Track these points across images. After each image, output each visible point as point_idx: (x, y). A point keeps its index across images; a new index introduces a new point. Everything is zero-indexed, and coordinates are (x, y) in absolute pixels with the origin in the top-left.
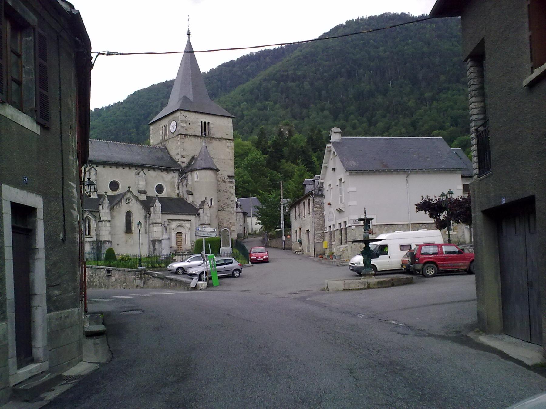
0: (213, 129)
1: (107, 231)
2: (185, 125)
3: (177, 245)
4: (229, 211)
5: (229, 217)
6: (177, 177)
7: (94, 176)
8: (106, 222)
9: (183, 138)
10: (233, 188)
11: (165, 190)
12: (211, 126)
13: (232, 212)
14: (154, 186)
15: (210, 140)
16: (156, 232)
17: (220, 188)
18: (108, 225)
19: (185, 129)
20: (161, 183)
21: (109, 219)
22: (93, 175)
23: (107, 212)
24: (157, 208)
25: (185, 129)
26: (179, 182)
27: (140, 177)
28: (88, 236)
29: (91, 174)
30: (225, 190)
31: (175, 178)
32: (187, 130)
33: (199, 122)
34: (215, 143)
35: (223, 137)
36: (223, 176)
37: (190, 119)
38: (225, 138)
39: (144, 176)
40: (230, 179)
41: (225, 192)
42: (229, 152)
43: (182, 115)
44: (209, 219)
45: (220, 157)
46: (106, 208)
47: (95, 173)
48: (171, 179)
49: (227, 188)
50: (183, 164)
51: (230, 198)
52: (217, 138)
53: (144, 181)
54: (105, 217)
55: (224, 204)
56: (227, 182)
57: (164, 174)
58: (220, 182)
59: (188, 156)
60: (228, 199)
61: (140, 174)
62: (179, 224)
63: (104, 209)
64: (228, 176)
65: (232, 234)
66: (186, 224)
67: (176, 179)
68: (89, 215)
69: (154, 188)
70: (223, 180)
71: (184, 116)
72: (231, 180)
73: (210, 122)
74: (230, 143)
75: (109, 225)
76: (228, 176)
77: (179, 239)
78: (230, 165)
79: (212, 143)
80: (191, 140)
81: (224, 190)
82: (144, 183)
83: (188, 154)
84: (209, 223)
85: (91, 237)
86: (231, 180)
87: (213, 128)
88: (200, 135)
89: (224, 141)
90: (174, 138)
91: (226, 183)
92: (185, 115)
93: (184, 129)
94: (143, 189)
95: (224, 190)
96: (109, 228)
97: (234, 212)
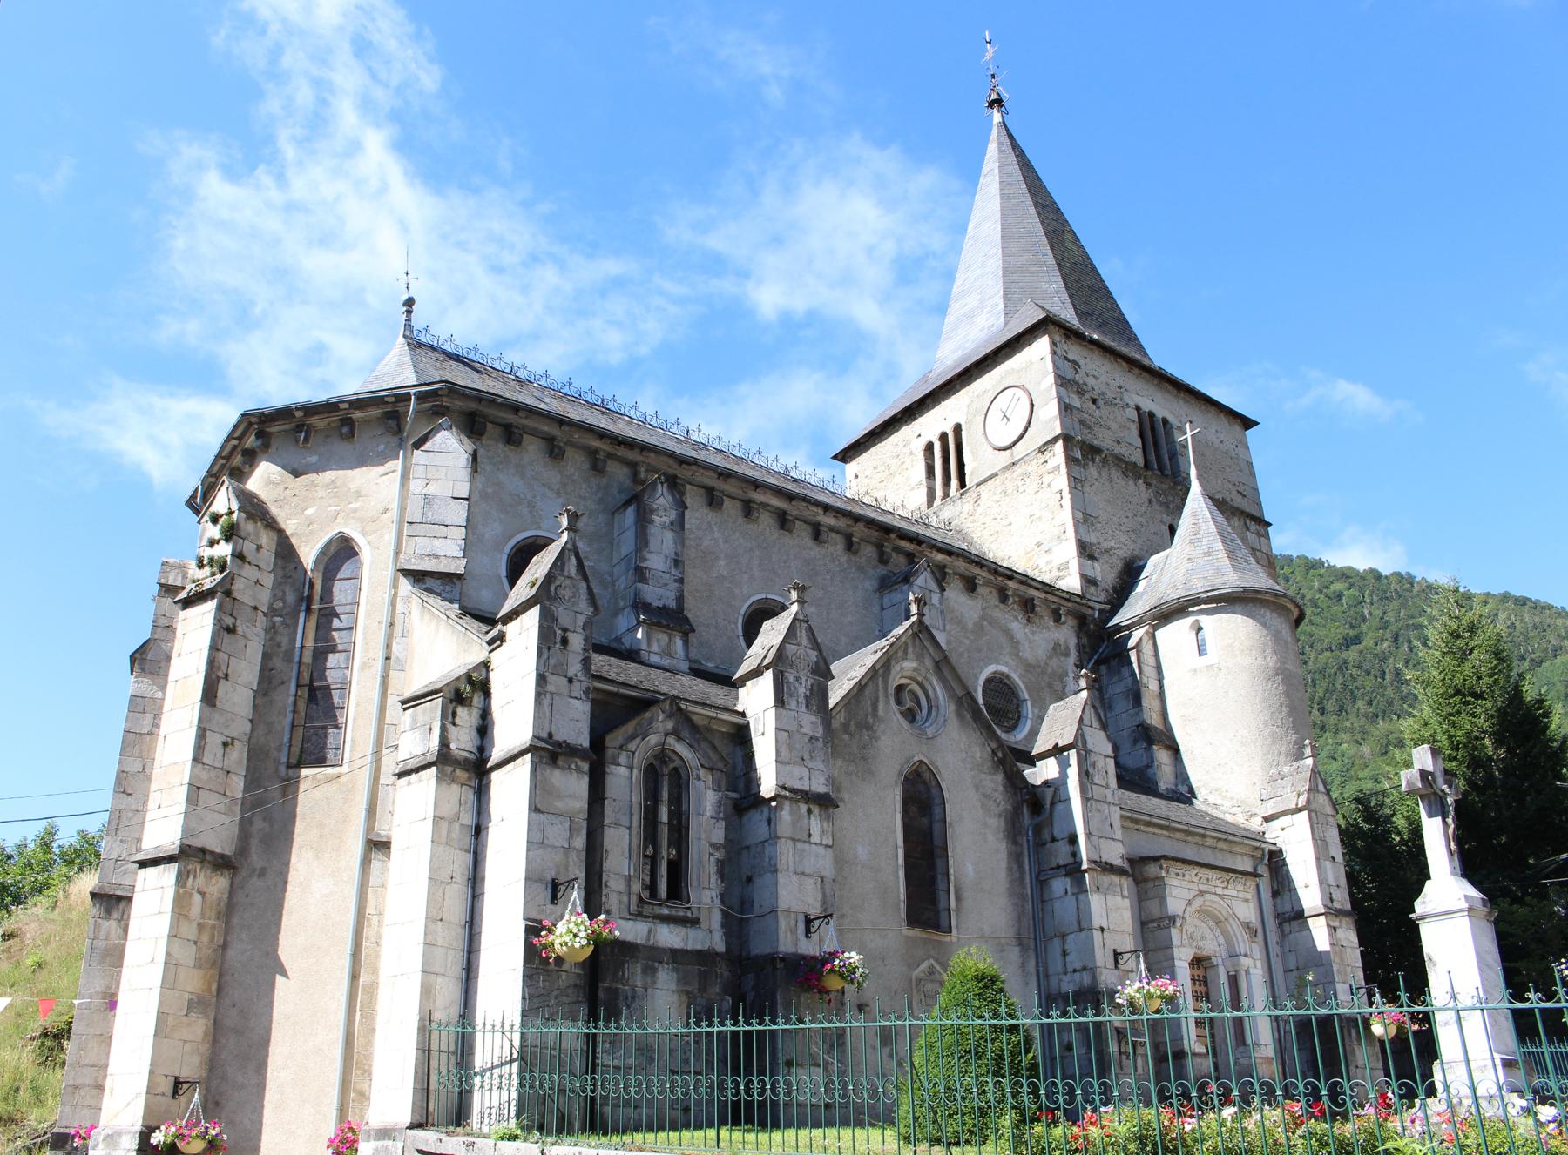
1: (811, 880)
7: (669, 536)
8: (803, 808)
16: (1102, 930)
18: (815, 838)
20: (1004, 669)
22: (663, 526)
28: (665, 911)
32: (1089, 428)
37: (1091, 381)
46: (802, 699)
47: (673, 515)
62: (1201, 893)
63: (793, 705)
66: (1234, 903)
71: (1066, 358)
85: (694, 922)
88: (1141, 462)
90: (1018, 470)
92: (1071, 357)
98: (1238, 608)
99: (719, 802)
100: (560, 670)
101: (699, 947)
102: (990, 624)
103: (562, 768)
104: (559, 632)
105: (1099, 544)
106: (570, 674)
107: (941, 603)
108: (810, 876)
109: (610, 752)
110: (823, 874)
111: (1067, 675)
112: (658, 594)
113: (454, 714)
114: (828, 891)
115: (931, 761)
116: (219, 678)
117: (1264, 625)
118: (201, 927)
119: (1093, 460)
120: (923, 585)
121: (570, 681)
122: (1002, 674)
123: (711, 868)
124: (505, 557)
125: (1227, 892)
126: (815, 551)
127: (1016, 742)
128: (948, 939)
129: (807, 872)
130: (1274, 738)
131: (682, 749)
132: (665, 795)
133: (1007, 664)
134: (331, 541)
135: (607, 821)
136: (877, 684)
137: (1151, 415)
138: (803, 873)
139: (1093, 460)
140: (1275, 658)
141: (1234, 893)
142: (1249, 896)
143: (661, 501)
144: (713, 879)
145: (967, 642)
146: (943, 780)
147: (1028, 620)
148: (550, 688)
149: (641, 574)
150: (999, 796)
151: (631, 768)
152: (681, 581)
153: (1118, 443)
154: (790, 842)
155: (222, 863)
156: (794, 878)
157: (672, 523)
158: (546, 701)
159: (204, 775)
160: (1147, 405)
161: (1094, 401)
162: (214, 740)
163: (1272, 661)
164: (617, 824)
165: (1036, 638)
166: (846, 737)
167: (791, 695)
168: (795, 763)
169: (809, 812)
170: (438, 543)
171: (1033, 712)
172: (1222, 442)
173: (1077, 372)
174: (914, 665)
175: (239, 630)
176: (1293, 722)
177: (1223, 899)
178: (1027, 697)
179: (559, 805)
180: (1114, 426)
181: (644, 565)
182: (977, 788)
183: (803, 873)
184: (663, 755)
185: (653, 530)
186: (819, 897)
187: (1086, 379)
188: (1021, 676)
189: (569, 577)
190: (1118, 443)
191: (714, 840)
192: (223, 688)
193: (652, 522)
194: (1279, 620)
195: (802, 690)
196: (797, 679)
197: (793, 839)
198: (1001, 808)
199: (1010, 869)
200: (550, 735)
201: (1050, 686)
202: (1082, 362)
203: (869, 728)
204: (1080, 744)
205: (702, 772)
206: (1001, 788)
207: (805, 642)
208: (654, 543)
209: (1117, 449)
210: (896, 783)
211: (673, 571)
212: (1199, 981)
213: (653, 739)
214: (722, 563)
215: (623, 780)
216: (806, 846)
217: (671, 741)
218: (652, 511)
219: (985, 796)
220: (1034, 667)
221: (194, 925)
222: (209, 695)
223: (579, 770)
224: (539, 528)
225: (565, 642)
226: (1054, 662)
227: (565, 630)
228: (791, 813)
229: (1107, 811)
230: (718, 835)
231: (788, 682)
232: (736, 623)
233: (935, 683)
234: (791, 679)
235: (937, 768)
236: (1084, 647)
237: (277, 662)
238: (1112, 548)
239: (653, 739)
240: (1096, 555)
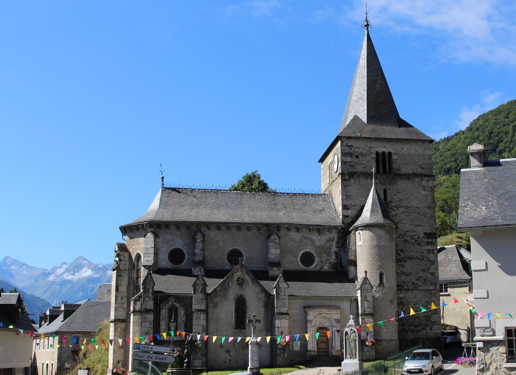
0: (398, 161)
1: (200, 326)
2: (349, 159)
3: (318, 348)
4: (426, 290)
5: (427, 300)
6: (336, 240)
7: (201, 244)
8: (199, 313)
9: (346, 180)
10: (433, 253)
11: (316, 259)
12: (394, 157)
13: (433, 292)
14: (298, 255)
15: (393, 179)
16: (278, 327)
17: (411, 254)
18: (202, 318)
19: (350, 166)
20: (308, 250)
21: (203, 308)
22: (199, 242)
23: (201, 297)
24: (281, 291)
25: (350, 166)
26: (340, 247)
27: (271, 242)
29: (197, 241)
30: (419, 257)
31: (333, 240)
32: (353, 166)
33: (372, 153)
34: (401, 184)
35: (415, 172)
36: (415, 233)
37: (357, 150)
38: (418, 173)
39: (277, 241)
40: (428, 238)
41: (420, 259)
42: (426, 196)
43: (344, 145)
44: (371, 306)
45: (409, 205)
46: (200, 292)
47: (202, 239)
48: (326, 243)
49: (423, 253)
50: (347, 219)
51: (429, 268)
52: (405, 175)
53: (279, 247)
54: (198, 306)
55: (417, 279)
56: (423, 244)
57: (315, 237)
58: (411, 244)
59: (354, 205)
60: (424, 270)
61: (273, 237)
62: (320, 314)
64: (425, 233)
65: (432, 329)
67: (335, 242)
68: (175, 302)
69: (297, 258)
70: (416, 241)
71: (347, 146)
72: (430, 240)
73: (392, 151)
74: (428, 180)
75: (203, 317)
76: (425, 233)
77: (323, 338)
78: (428, 215)
79: (395, 183)
80: (359, 182)
81: (417, 257)
82: (278, 251)
83: (354, 203)
84: (372, 312)
86: (430, 240)
87: (397, 159)
89: (417, 180)
91: (421, 245)
92: (349, 145)
93: (348, 166)
94: (277, 260)
95: (417, 257)
96: (204, 323)
97: (436, 291)
98: (367, 229)
99: (184, 313)
100: (147, 296)
101: (180, 340)
102: (305, 239)
103: (148, 314)
104: (147, 290)
105: (352, 204)
106: (150, 296)
107: (279, 241)
108: (200, 325)
109: (161, 307)
110: (203, 324)
111: (332, 246)
112: (198, 258)
113: (136, 303)
114: (204, 328)
115: (243, 294)
116: (118, 286)
117: (374, 233)
118: (120, 333)
119: (353, 177)
120: (273, 238)
121: (150, 298)
122: (308, 251)
123: (183, 325)
124: (167, 254)
125: (330, 312)
126: (248, 233)
127: (311, 269)
128: (245, 331)
129: (200, 324)
130: (373, 264)
131: (177, 304)
132: (173, 313)
133: (309, 249)
134: (137, 254)
135: (161, 320)
136: (229, 280)
137: (383, 153)
138: (199, 325)
139: (353, 177)
140: (376, 242)
141: (333, 312)
142: (339, 313)
143: (199, 236)
144: (183, 327)
145: (296, 245)
146: (246, 297)
147: (319, 234)
148: (146, 300)
149: (194, 255)
150: (263, 298)
151: (165, 309)
152: (204, 254)
153: (366, 168)
154: (196, 320)
155: (123, 321)
156: (197, 326)
157: (201, 241)
158: (145, 302)
159: (118, 305)
160: (381, 150)
161: (357, 157)
162: (119, 298)
163: (375, 243)
164: (163, 320)
165: (322, 238)
166: (220, 293)
167: (197, 291)
168: (197, 304)
169: (200, 313)
170: (149, 258)
171: (318, 260)
172: (417, 151)
173: (351, 149)
174: (241, 273)
175: (122, 275)
176: (379, 260)
178: (316, 256)
179: (148, 320)
180: (364, 162)
181: (195, 252)
182: (256, 297)
183: (199, 325)
184: (173, 306)
185: (197, 244)
186: (202, 329)
187: (354, 150)
188: (314, 251)
189: (149, 279)
190: (366, 168)
191: (183, 320)
192: (120, 288)
193: (196, 242)
194: (380, 230)
195: (200, 290)
196: (199, 288)
197: (197, 319)
198: (263, 301)
199: (265, 314)
200: (146, 308)
201: (325, 251)
202: (354, 145)
203: (227, 290)
204: (277, 287)
205: (181, 308)
206: (264, 296)
207: (201, 280)
208: (197, 247)
209: (365, 170)
210: (233, 300)
211: (202, 252)
213: (170, 303)
214: (221, 243)
215: (164, 312)
216: (200, 320)
217: (174, 303)
218: (197, 239)
219: (259, 299)
220: (319, 247)
221: (119, 333)
222: (117, 290)
223: (151, 314)
224: (175, 246)
225: (148, 291)
226: (328, 244)
227: (148, 289)
228: (196, 314)
229: (284, 301)
230: (184, 319)
231: (197, 289)
232: (225, 257)
233: (247, 276)
234: (197, 288)
235: (245, 295)
236: (341, 237)
237: (130, 280)
238: (357, 204)
239: (170, 303)
240: (350, 208)
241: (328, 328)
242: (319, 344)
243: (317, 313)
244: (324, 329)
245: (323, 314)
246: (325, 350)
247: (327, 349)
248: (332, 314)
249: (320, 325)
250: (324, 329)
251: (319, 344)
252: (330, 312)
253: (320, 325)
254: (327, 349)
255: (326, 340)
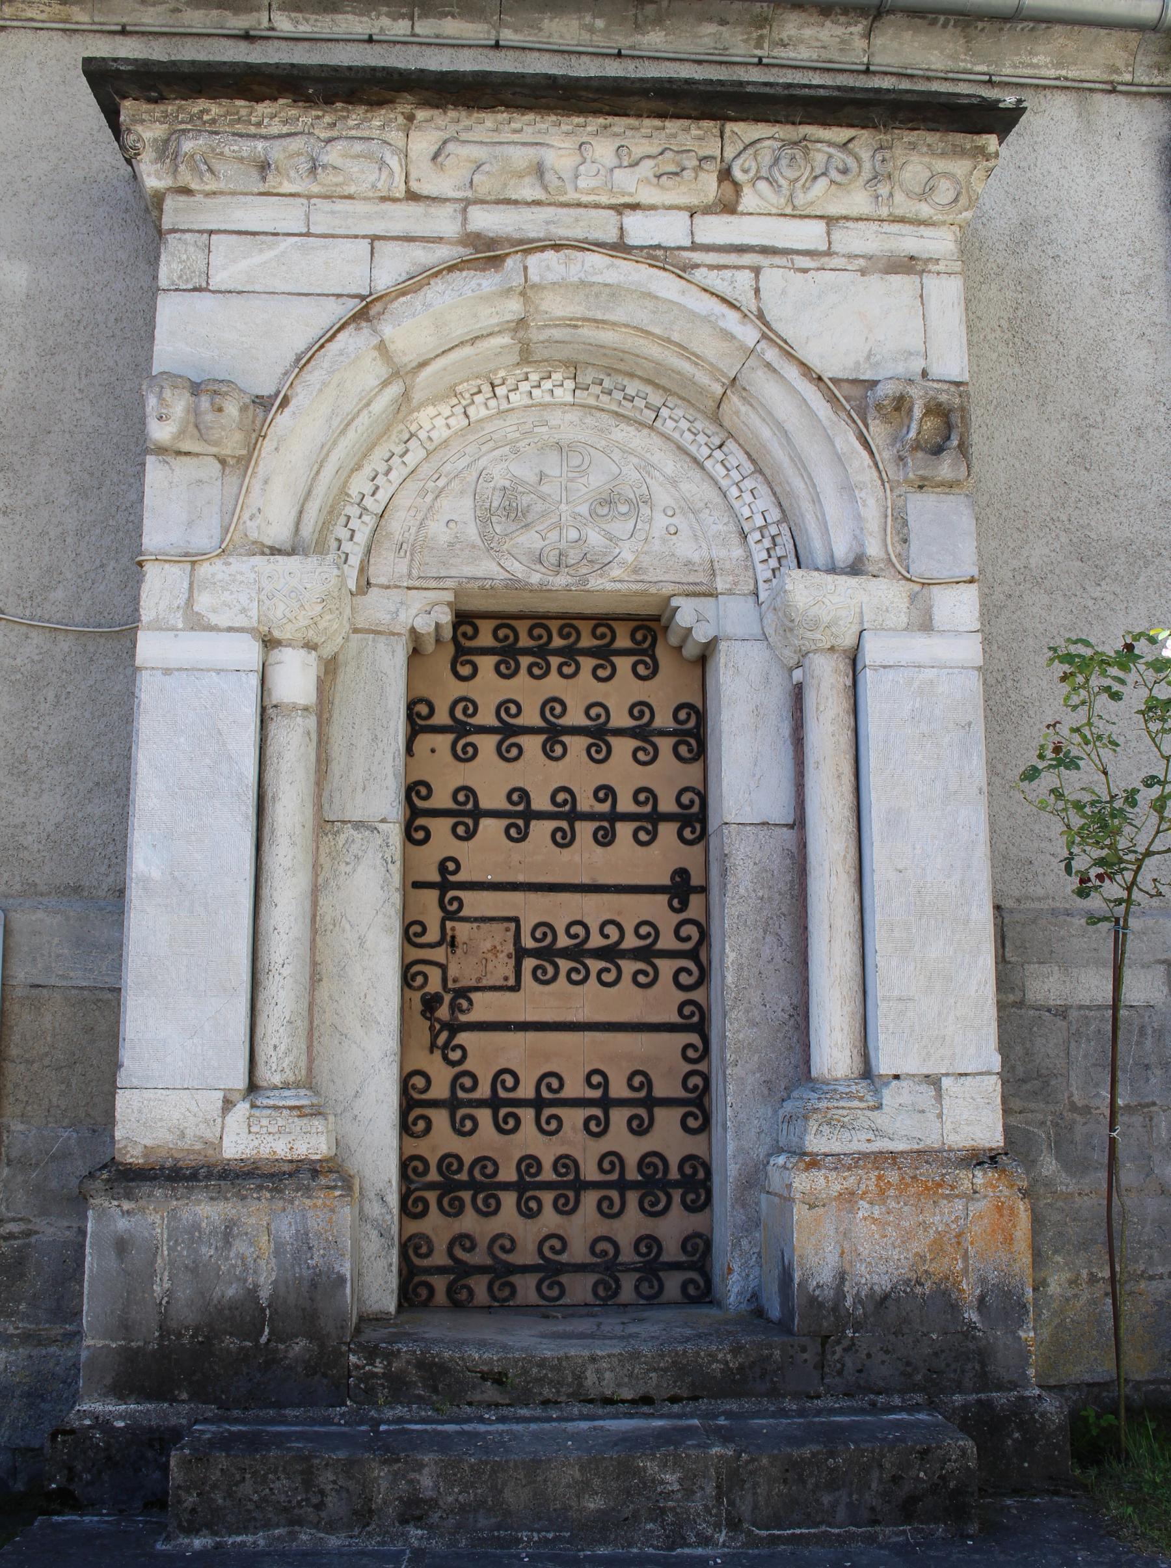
141: (810, 234)
177: (683, 270)
212: (643, 733)
241: (686, 613)
242: (484, 1007)
243: (405, 217)
244: (604, 654)
245: (545, 266)
246: (632, 1149)
247: (667, 1120)
248: (774, 277)
249: (490, 545)
250: (604, 654)
251: (484, 1007)
252: (716, 229)
253: (490, 545)
254: (667, 1120)
255: (656, 908)
